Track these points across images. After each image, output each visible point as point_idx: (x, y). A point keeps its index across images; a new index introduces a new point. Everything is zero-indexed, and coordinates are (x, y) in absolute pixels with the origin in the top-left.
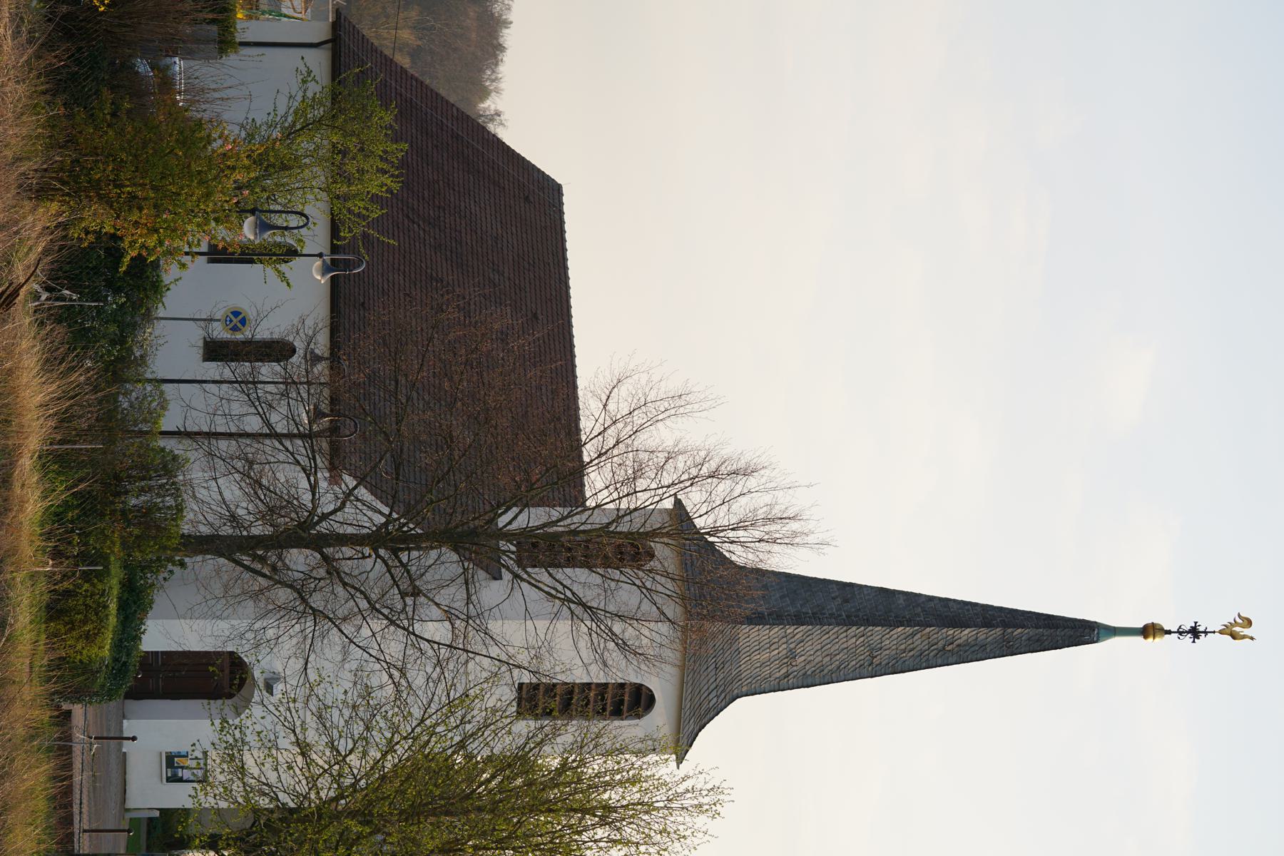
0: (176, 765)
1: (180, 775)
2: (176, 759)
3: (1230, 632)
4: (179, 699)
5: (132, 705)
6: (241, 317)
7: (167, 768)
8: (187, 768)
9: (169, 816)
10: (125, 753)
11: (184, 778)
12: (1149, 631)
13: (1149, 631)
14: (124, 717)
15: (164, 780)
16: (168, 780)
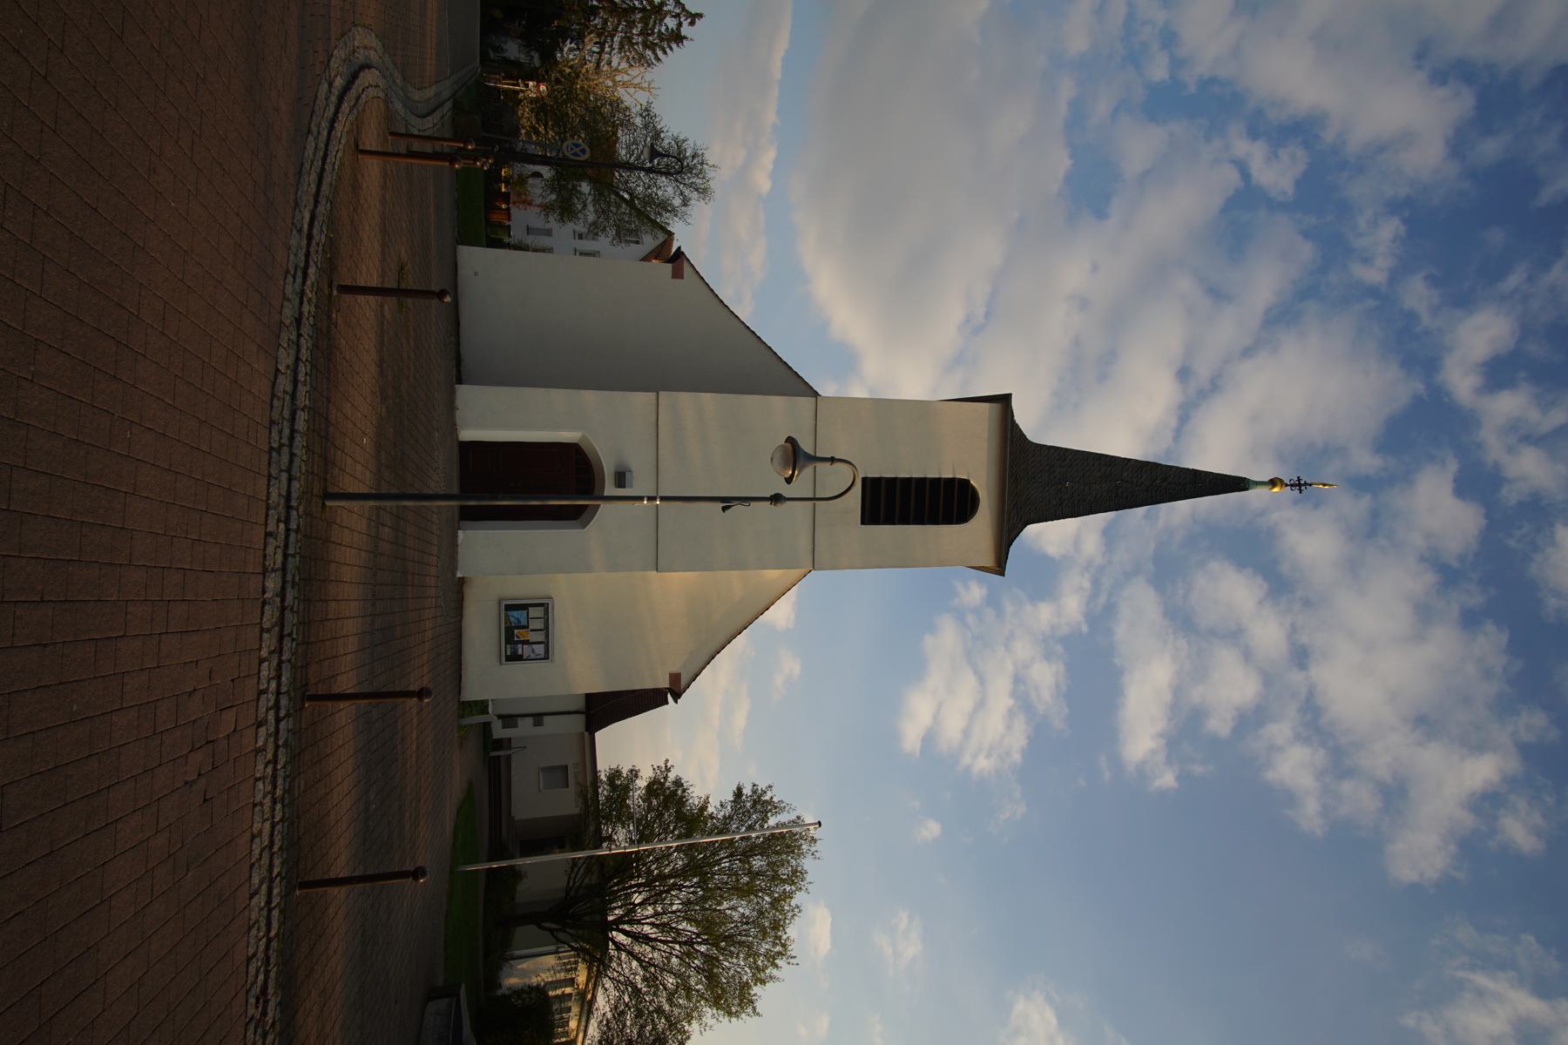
0: (516, 639)
1: (520, 652)
2: (516, 631)
8: (527, 642)
10: (462, 581)
14: (459, 529)
15: (504, 659)
16: (509, 659)
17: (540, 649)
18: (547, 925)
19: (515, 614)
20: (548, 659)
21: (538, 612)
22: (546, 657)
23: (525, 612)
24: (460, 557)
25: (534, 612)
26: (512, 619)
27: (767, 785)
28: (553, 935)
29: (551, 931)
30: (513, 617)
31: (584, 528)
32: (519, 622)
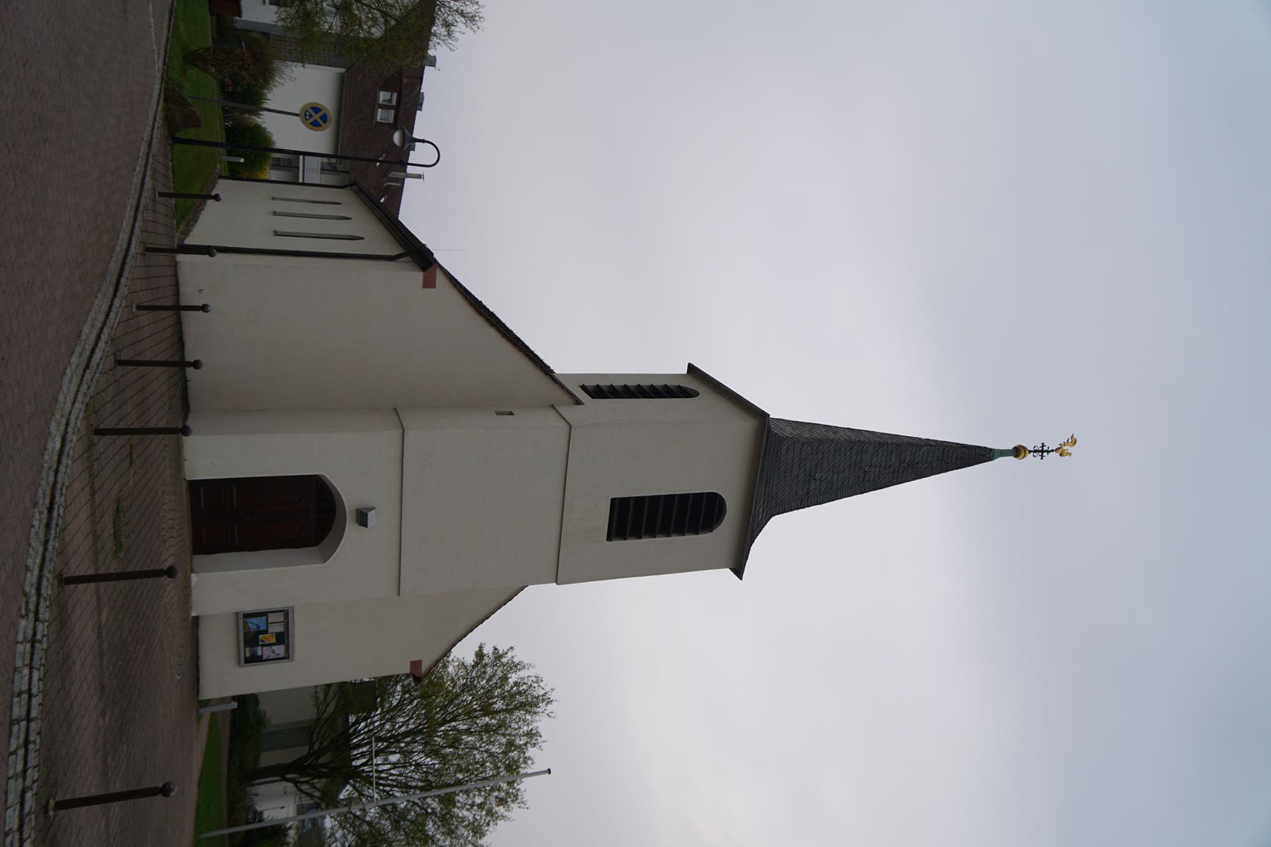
1: (259, 653)
3: (1061, 451)
4: (258, 550)
5: (200, 559)
6: (321, 114)
7: (245, 648)
9: (246, 703)
10: (197, 619)
11: (264, 658)
12: (1018, 452)
13: (1018, 452)
14: (192, 571)
15: (243, 661)
17: (280, 650)
18: (289, 776)
19: (255, 620)
20: (288, 658)
21: (279, 617)
22: (287, 657)
23: (264, 618)
24: (194, 598)
25: (272, 618)
26: (251, 625)
27: (508, 647)
28: (297, 787)
29: (295, 782)
30: (252, 623)
31: (324, 562)
32: (258, 627)
